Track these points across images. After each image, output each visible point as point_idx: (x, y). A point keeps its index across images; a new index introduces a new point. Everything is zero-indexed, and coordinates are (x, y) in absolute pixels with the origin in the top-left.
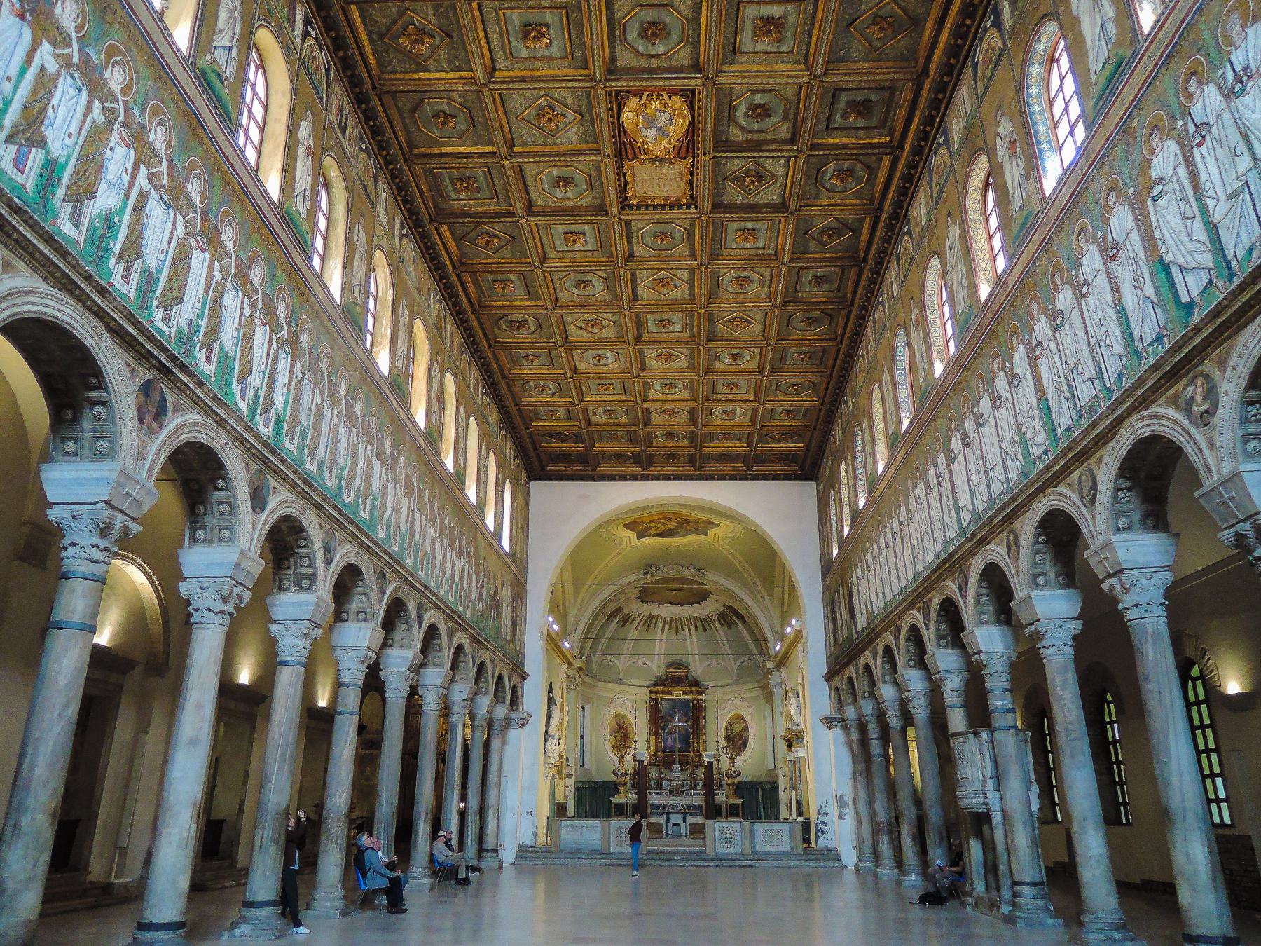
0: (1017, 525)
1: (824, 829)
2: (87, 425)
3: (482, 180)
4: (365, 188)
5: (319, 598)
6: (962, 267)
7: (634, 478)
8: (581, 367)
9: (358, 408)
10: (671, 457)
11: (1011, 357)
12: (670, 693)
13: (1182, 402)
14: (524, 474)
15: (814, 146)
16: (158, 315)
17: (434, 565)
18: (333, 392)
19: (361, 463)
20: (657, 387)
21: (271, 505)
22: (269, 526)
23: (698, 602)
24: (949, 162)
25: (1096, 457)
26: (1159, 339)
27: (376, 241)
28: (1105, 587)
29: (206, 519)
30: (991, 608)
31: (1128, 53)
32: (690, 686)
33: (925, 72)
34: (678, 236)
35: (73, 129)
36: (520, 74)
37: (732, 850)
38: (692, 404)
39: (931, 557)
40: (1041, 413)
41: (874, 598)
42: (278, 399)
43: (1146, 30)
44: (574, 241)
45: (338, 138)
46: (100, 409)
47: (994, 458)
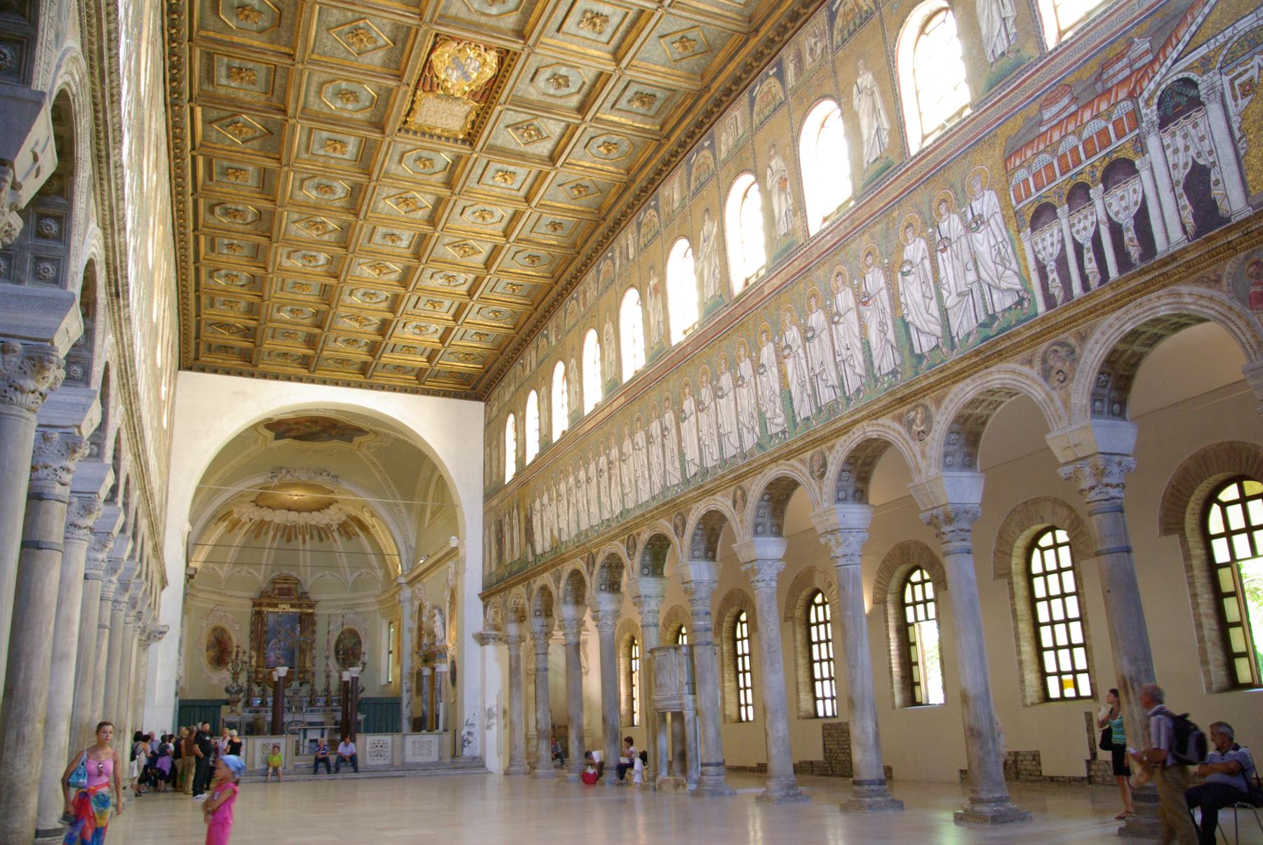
0: (746, 483)
1: (470, 739)
6: (716, 260)
7: (300, 380)
10: (342, 362)
11: (760, 350)
12: (276, 605)
13: (905, 420)
15: (596, 119)
20: (359, 294)
23: (318, 510)
24: (712, 167)
25: (829, 444)
26: (894, 373)
28: (822, 540)
30: (702, 546)
31: (897, 162)
32: (299, 598)
33: (707, 88)
34: (439, 165)
37: (382, 762)
38: (389, 316)
39: (645, 497)
40: (783, 401)
41: (563, 525)
43: (913, 153)
47: (729, 426)
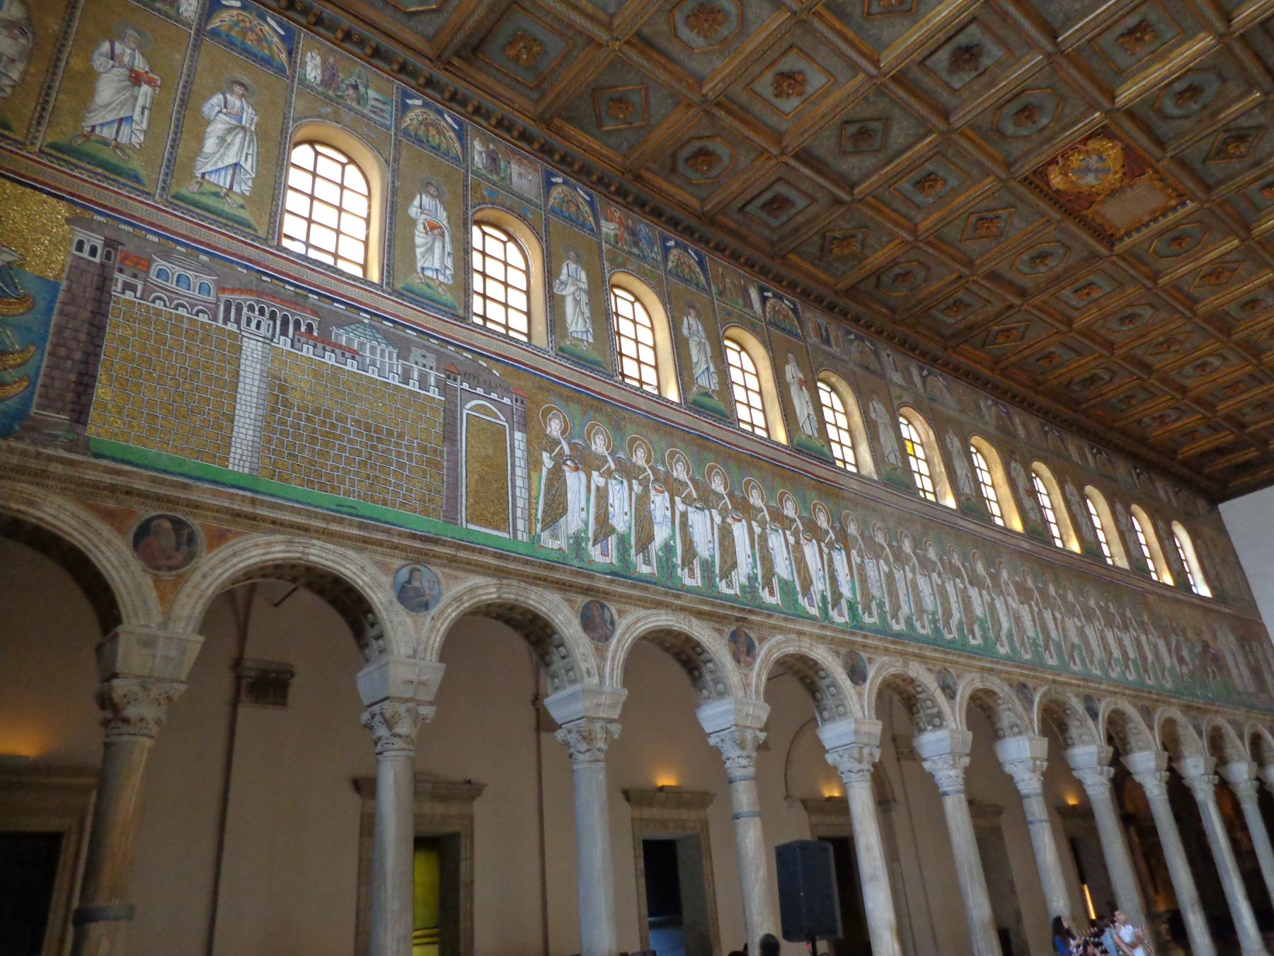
2: (708, 677)
3: (967, 299)
4: (867, 368)
5: (952, 731)
8: (1188, 383)
9: (932, 554)
14: (1201, 504)
16: (723, 587)
17: (1092, 654)
18: (899, 557)
19: (953, 599)
21: (871, 675)
22: (875, 691)
27: (896, 402)
29: (825, 702)
35: (626, 509)
36: (937, 216)
42: (845, 590)
44: (1088, 294)
45: (824, 352)
46: (710, 665)
